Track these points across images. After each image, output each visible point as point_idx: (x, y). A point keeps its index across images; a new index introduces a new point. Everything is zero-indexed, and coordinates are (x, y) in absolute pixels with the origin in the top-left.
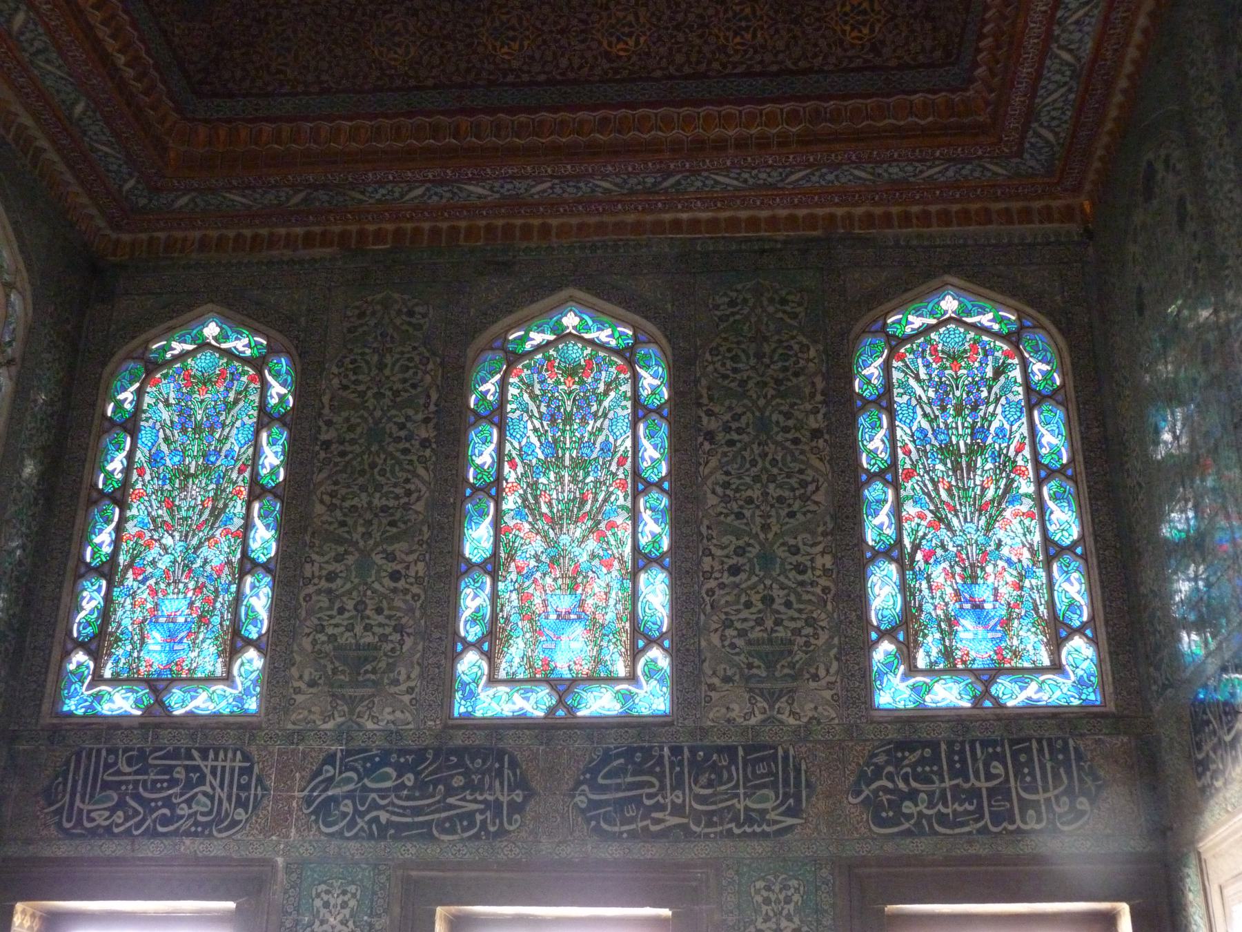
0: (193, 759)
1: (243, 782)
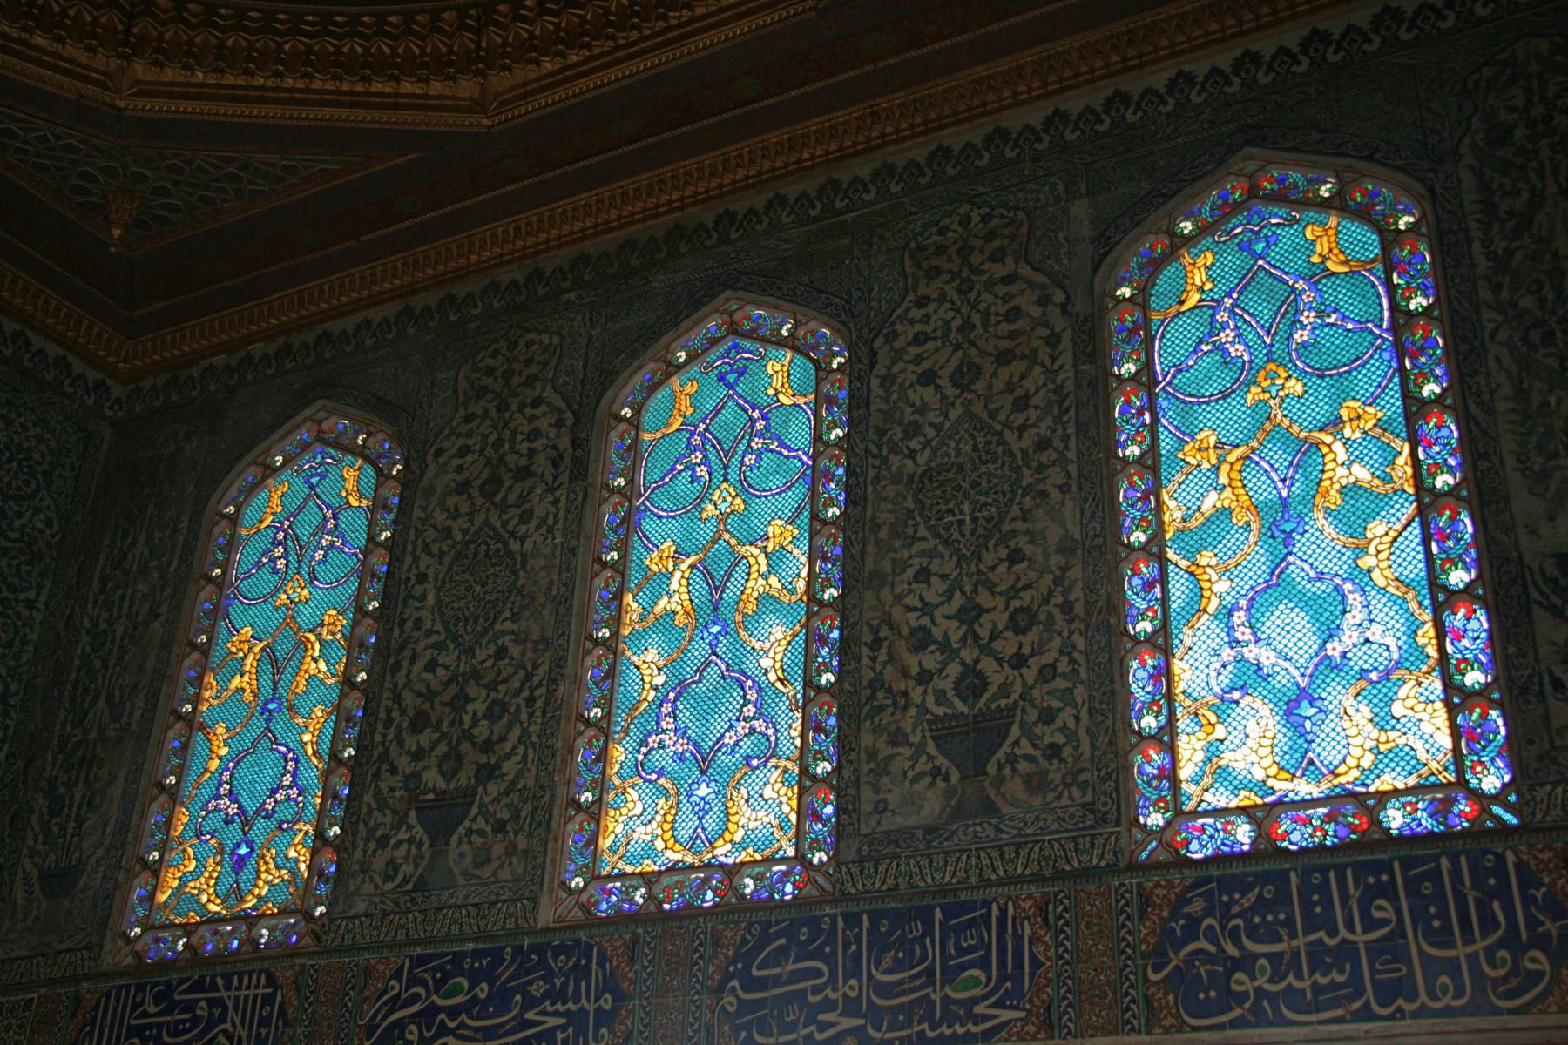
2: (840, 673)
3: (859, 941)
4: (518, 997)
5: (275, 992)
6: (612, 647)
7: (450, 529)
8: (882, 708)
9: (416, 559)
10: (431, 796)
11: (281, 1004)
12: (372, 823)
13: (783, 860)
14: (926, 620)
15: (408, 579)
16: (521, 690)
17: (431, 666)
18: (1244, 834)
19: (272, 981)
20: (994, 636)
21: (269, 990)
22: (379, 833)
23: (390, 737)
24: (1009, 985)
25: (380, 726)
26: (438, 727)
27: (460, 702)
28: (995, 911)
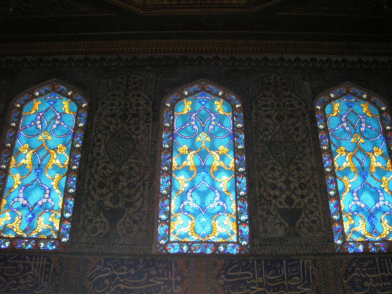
0: (26, 260)
1: (47, 270)
3: (262, 268)
4: (146, 274)
5: (51, 264)
7: (109, 127)
8: (263, 204)
9: (96, 134)
10: (108, 209)
11: (54, 268)
12: (86, 214)
13: (232, 243)
14: (275, 182)
15: (94, 140)
16: (139, 181)
17: (105, 168)
18: (361, 248)
19: (48, 260)
20: (295, 189)
21: (49, 263)
22: (89, 218)
23: (90, 188)
24: (306, 281)
25: (86, 185)
26: (109, 188)
27: (117, 181)
28: (301, 262)
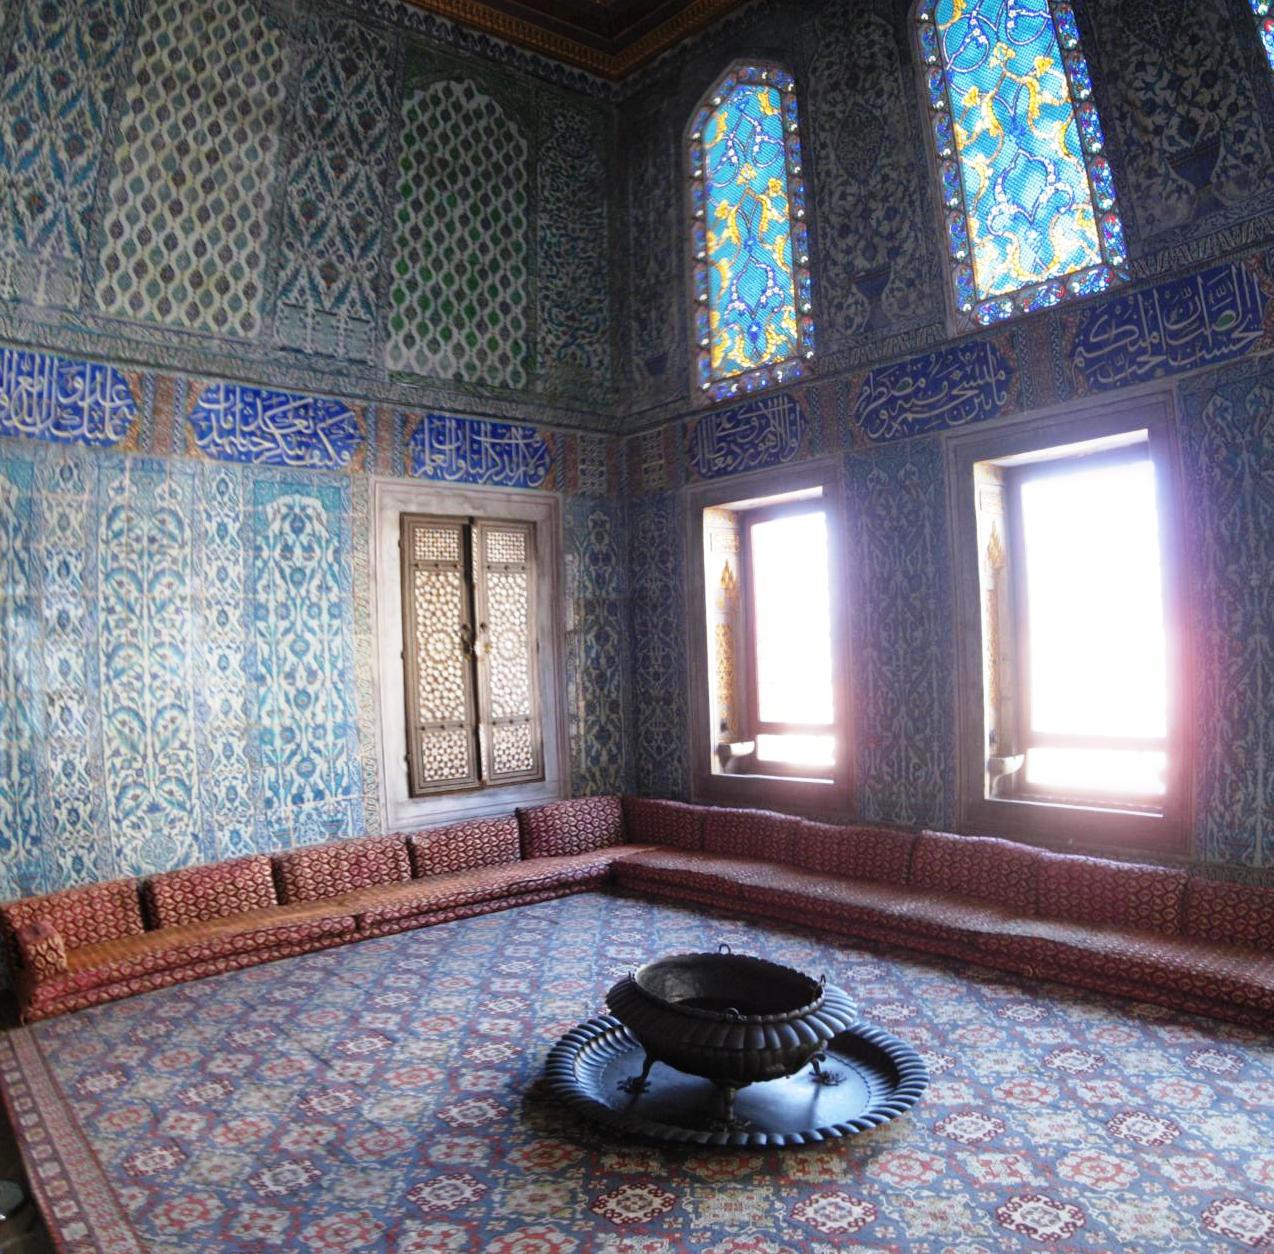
2: (1105, 140)
6: (955, 159)
8: (1136, 157)
17: (843, 196)
19: (791, 400)
26: (857, 231)
27: (866, 214)
